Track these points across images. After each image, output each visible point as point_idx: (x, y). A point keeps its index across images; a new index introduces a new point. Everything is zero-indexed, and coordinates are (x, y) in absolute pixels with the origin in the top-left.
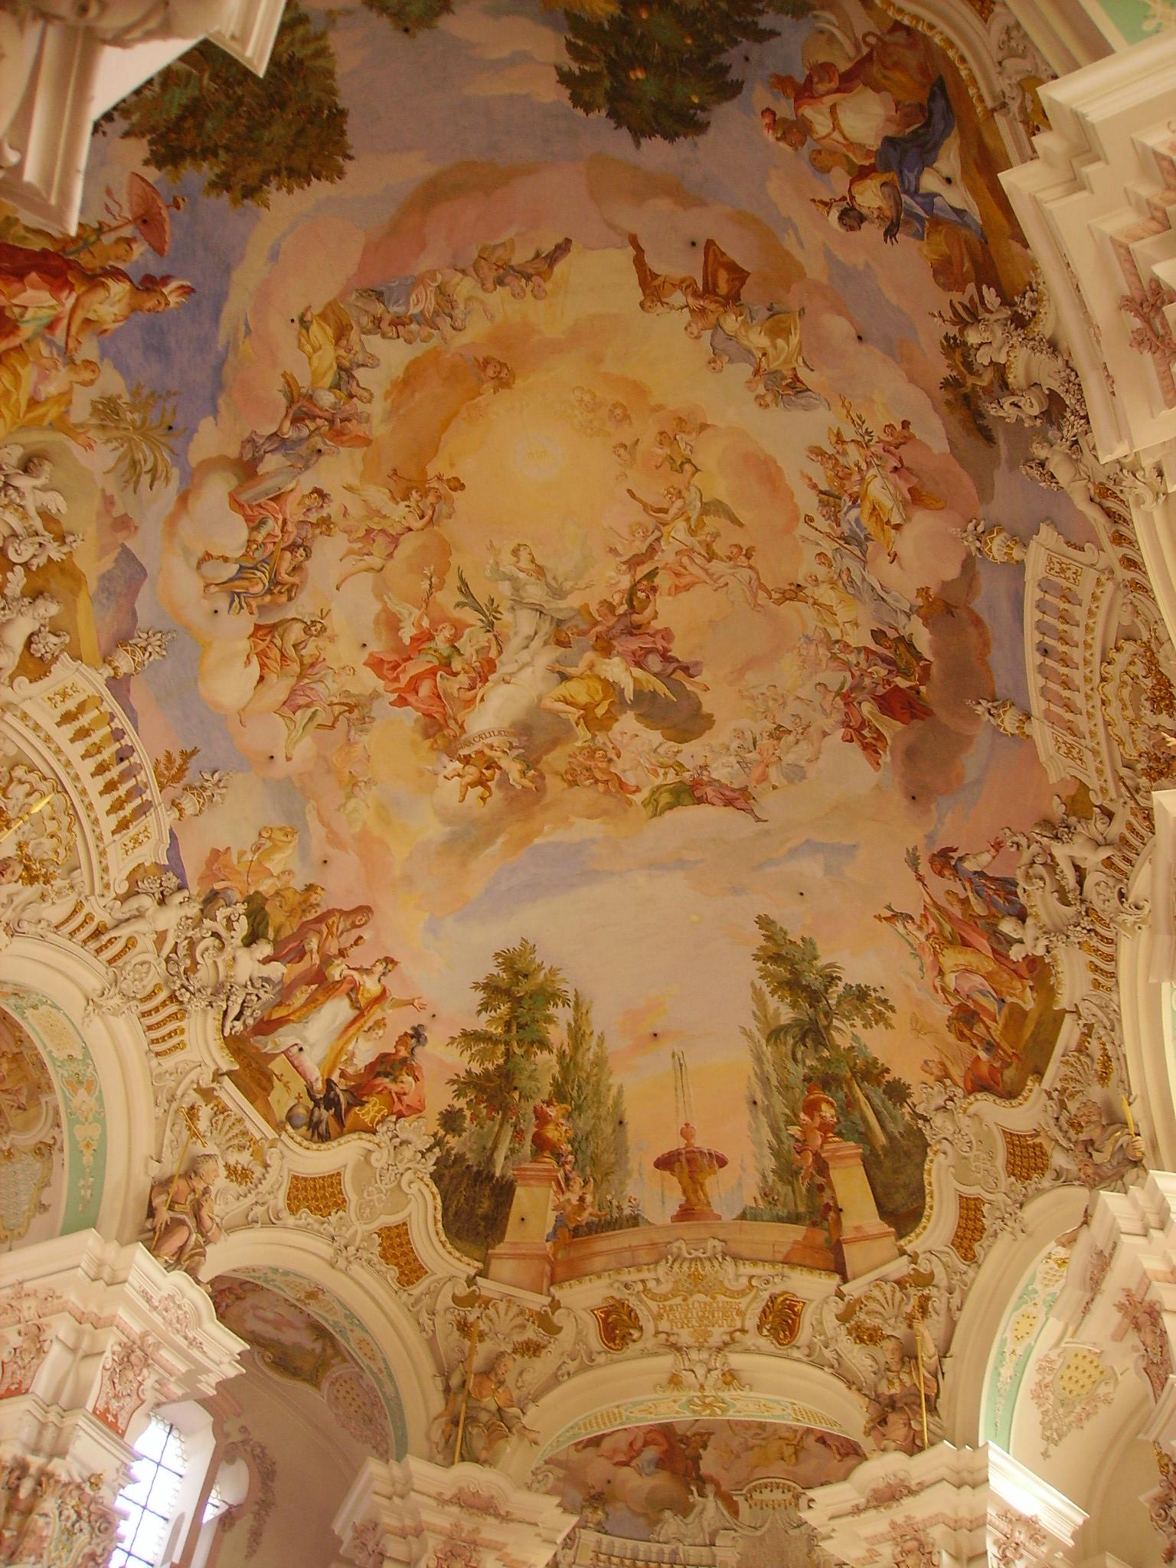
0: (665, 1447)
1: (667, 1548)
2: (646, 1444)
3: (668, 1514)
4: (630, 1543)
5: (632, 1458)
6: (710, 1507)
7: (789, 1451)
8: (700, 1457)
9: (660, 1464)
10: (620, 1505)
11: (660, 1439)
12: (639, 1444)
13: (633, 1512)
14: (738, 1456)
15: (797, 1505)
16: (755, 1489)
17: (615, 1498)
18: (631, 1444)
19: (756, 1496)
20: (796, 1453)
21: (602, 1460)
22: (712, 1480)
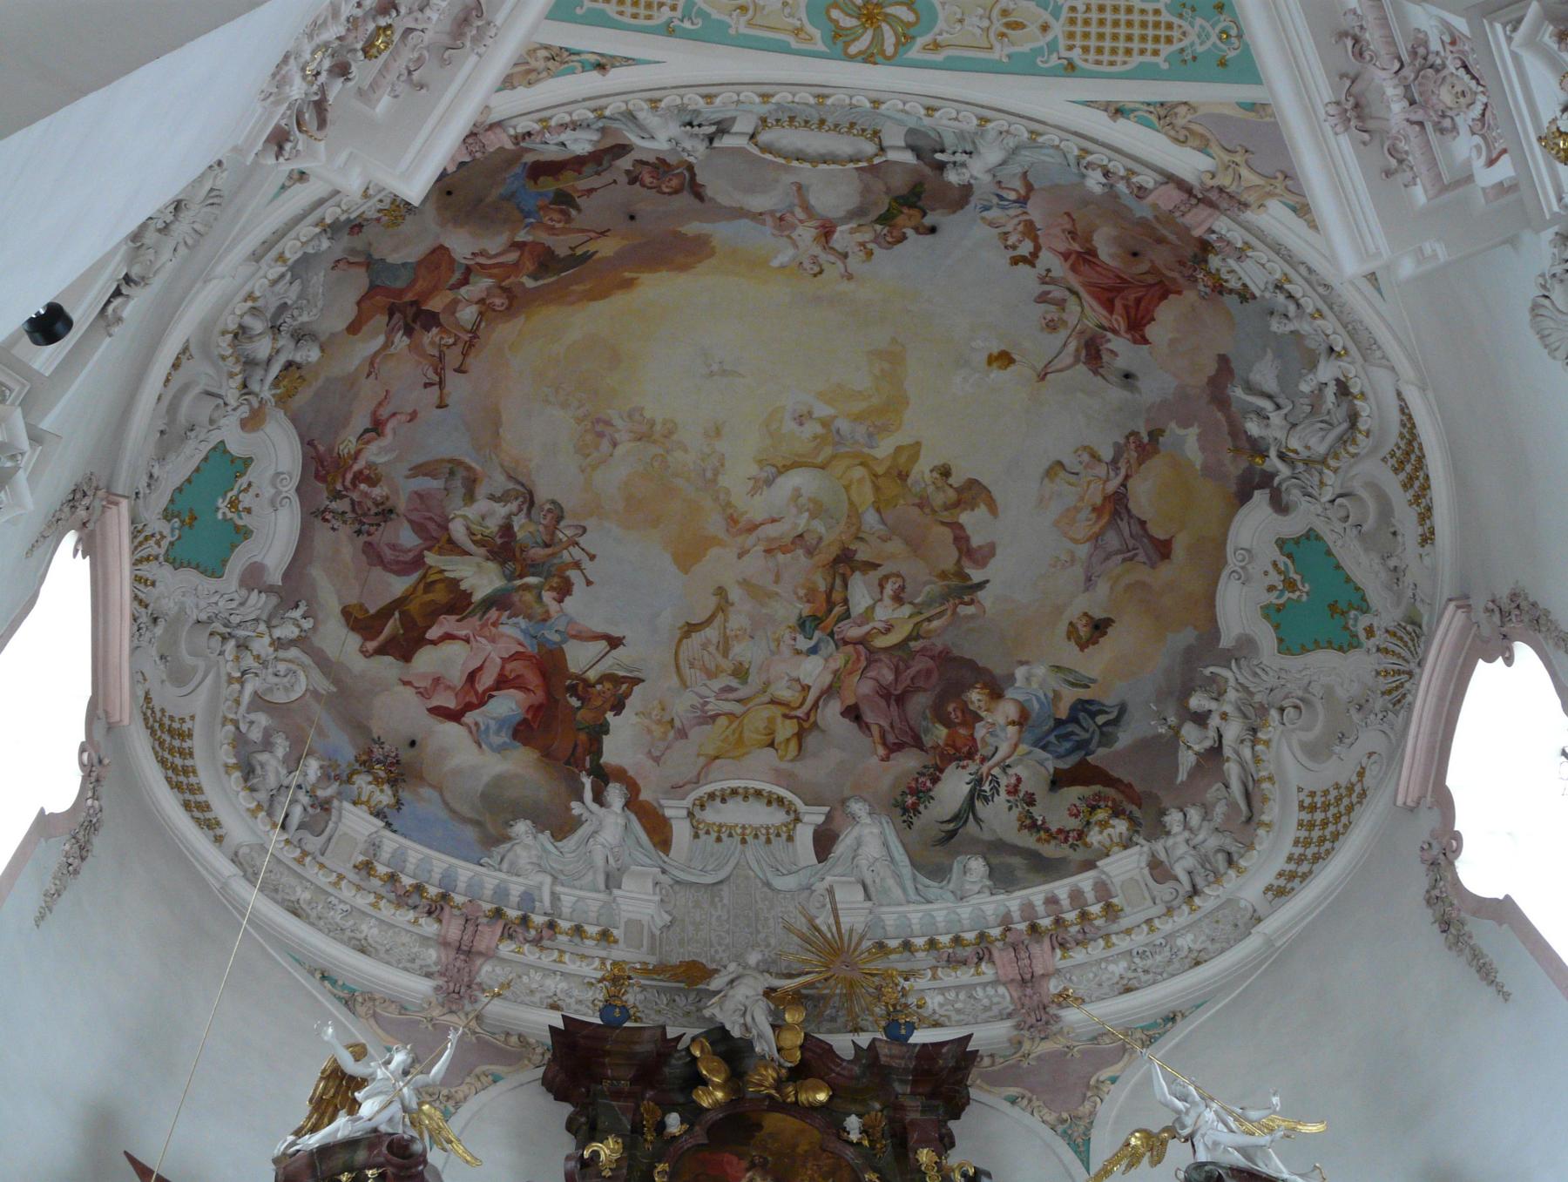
0: (539, 697)
1: (516, 889)
2: (502, 683)
3: (522, 827)
4: (440, 862)
5: (469, 707)
6: (608, 824)
7: (786, 730)
8: (604, 728)
9: (523, 732)
10: (425, 791)
11: (533, 679)
12: (486, 680)
13: (453, 811)
14: (683, 734)
15: (790, 839)
16: (712, 796)
17: (420, 778)
18: (472, 677)
19: (710, 815)
20: (800, 736)
21: (408, 692)
22: (621, 775)
